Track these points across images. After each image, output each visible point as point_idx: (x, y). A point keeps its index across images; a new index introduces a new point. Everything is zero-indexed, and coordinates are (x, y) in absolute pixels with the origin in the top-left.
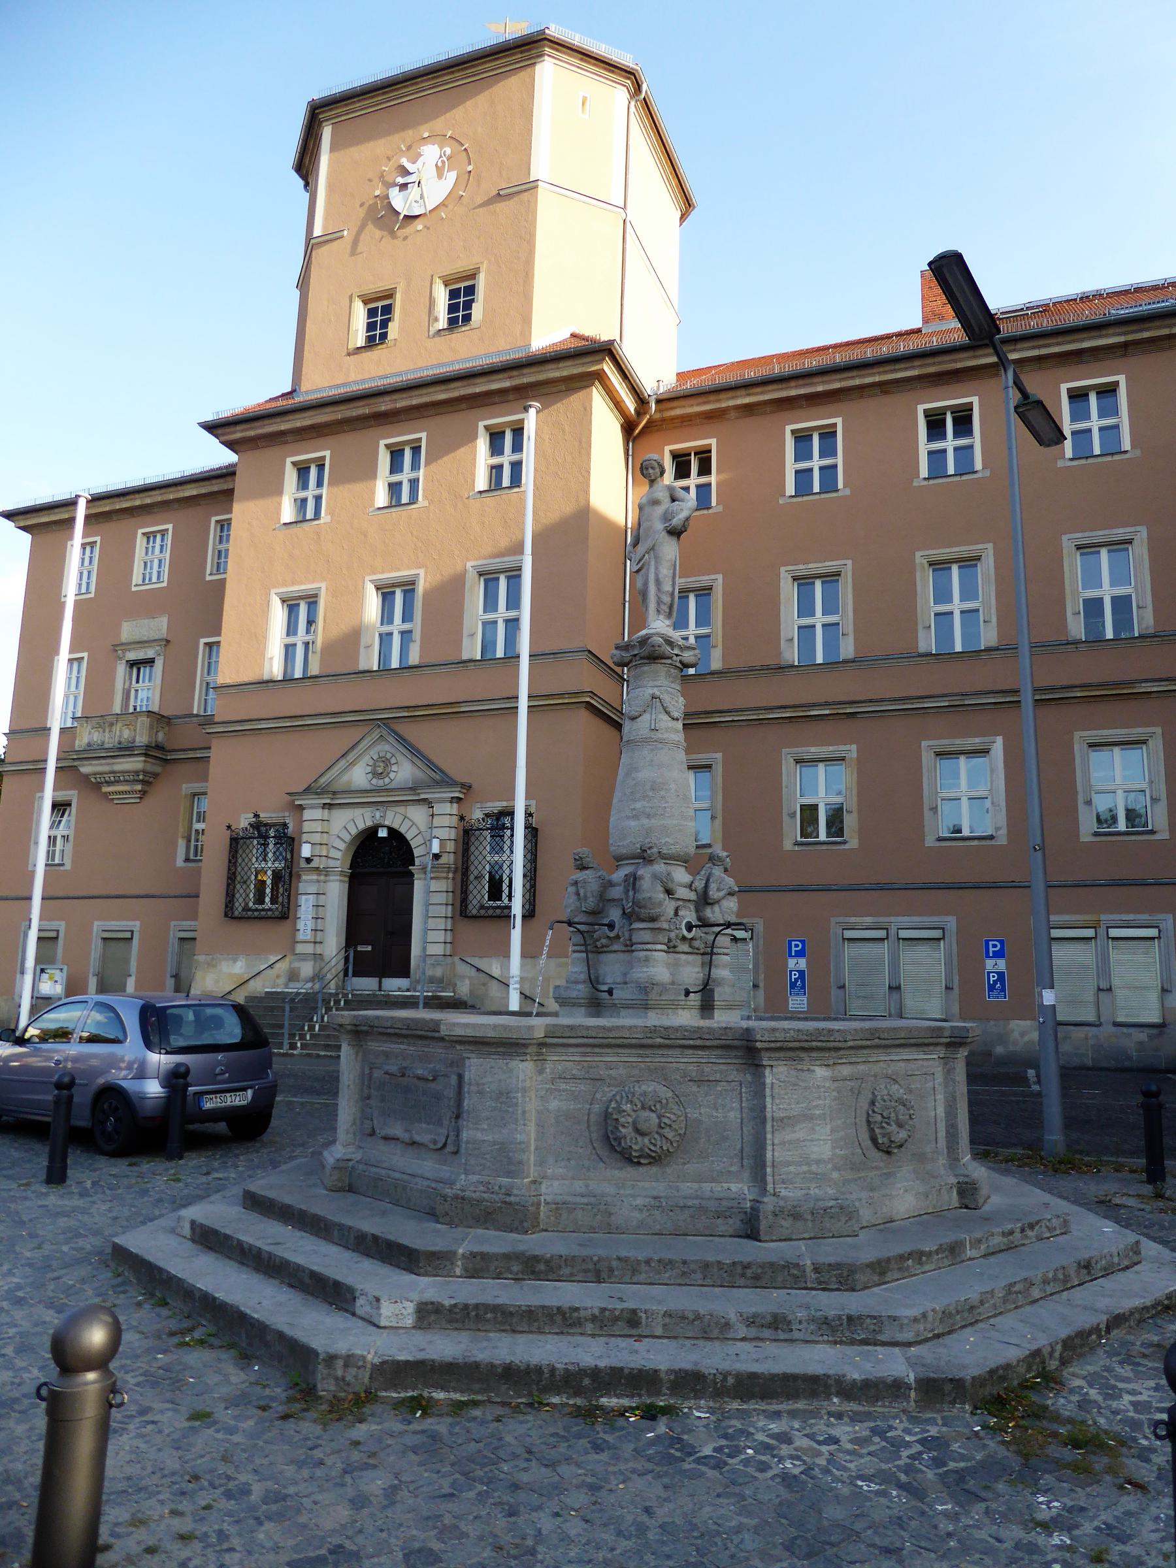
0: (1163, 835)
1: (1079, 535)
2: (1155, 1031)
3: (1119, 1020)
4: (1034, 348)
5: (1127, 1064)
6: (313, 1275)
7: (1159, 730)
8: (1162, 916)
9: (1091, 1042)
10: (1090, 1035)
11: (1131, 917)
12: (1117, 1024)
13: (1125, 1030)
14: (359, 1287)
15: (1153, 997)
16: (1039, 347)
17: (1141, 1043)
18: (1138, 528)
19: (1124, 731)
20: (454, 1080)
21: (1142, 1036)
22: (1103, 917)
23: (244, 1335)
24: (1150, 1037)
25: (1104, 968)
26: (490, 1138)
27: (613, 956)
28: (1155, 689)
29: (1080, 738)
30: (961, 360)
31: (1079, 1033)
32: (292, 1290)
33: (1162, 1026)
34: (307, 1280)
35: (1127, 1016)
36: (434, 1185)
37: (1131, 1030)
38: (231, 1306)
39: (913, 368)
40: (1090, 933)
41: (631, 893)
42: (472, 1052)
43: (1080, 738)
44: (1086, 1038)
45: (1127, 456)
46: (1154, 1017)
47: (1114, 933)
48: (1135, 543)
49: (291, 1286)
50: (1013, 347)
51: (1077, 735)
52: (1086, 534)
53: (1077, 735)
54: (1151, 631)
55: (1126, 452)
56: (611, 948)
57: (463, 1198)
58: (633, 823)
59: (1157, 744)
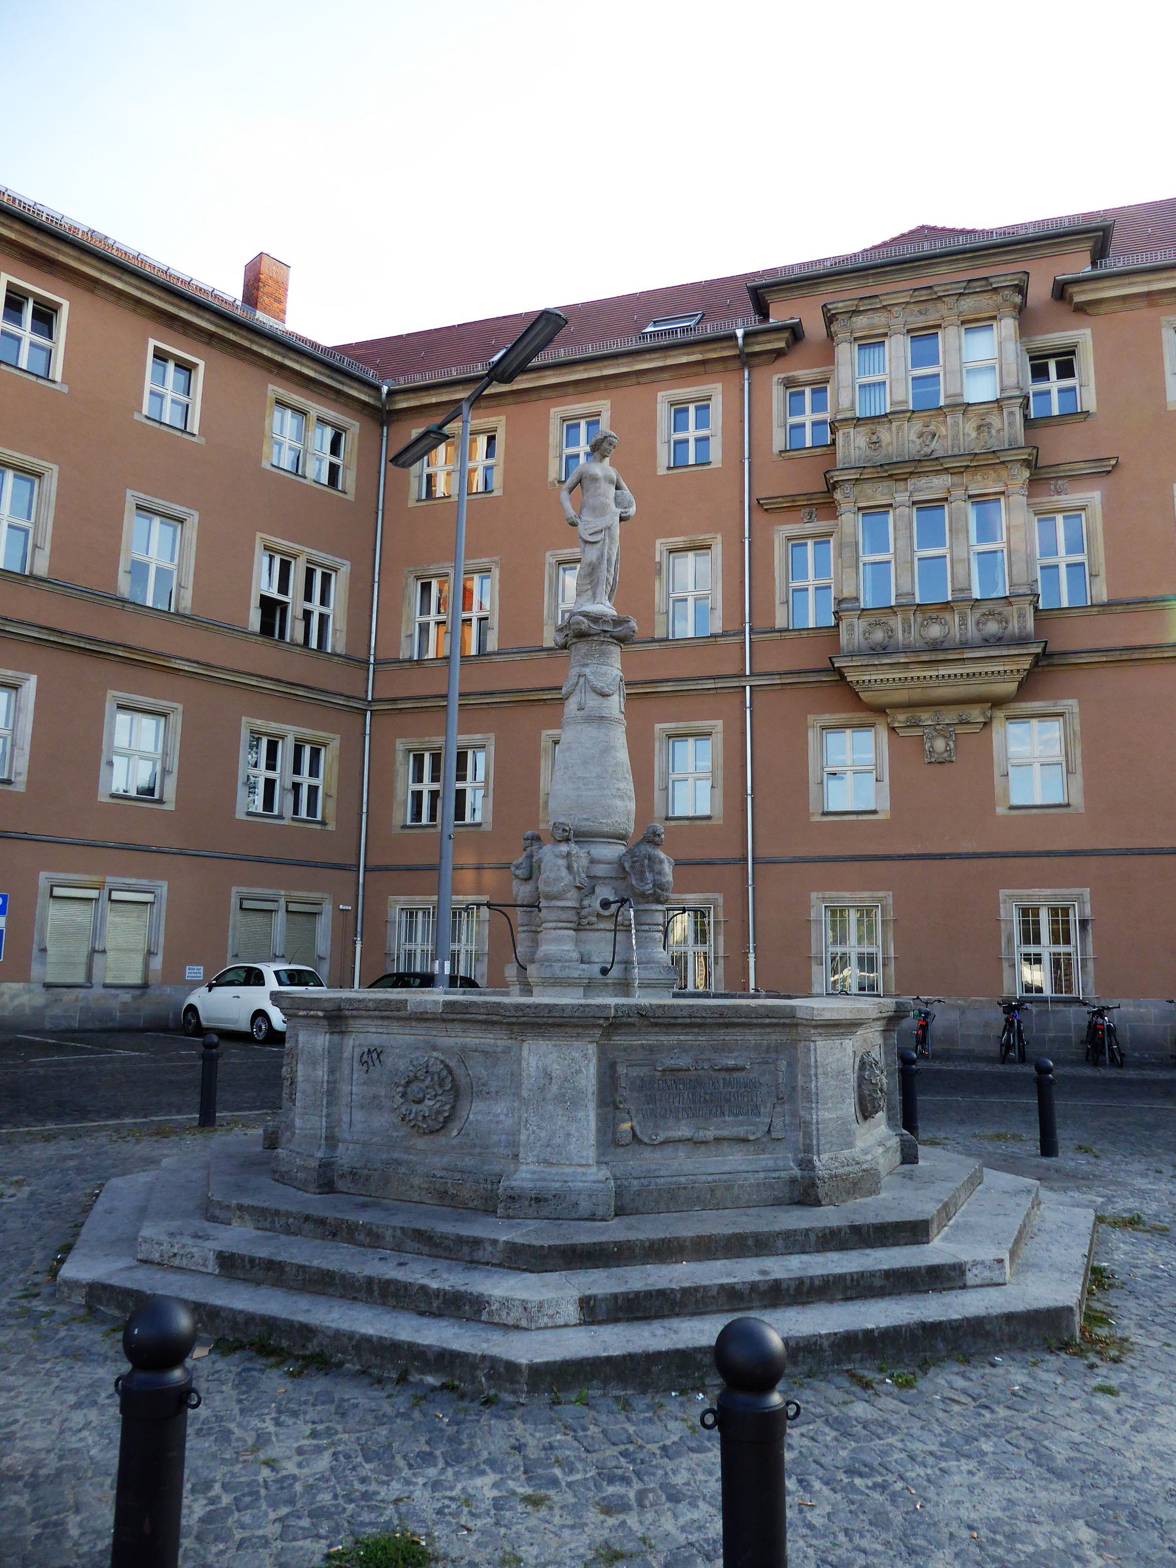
0: (170, 806)
1: (142, 495)
2: (137, 992)
3: (108, 981)
4: (138, 288)
5: (110, 1025)
6: (889, 1274)
7: (180, 707)
8: (159, 883)
9: (80, 1004)
10: (81, 996)
11: (133, 881)
12: (106, 986)
13: (113, 991)
14: (964, 1258)
15: (138, 961)
16: (143, 291)
17: (125, 1003)
18: (192, 512)
19: (151, 700)
20: (783, 1065)
21: (126, 996)
22: (109, 879)
23: (941, 1345)
24: (135, 998)
25: (97, 930)
26: (834, 1116)
27: (597, 934)
28: (186, 668)
29: (113, 696)
30: (65, 254)
31: (69, 996)
32: (849, 1303)
33: (145, 986)
34: (878, 1282)
35: (114, 977)
36: (776, 1174)
37: (118, 991)
38: (908, 1326)
39: (10, 228)
40: (93, 894)
41: (649, 875)
42: (820, 1034)
43: (113, 696)
44: (76, 1000)
45: (193, 439)
46: (135, 979)
47: (116, 895)
48: (187, 524)
49: (847, 1299)
50: (119, 275)
51: (111, 693)
52: (148, 498)
53: (111, 693)
54: (188, 612)
55: (193, 435)
56: (595, 927)
57: (836, 1176)
58: (619, 803)
59: (176, 720)
